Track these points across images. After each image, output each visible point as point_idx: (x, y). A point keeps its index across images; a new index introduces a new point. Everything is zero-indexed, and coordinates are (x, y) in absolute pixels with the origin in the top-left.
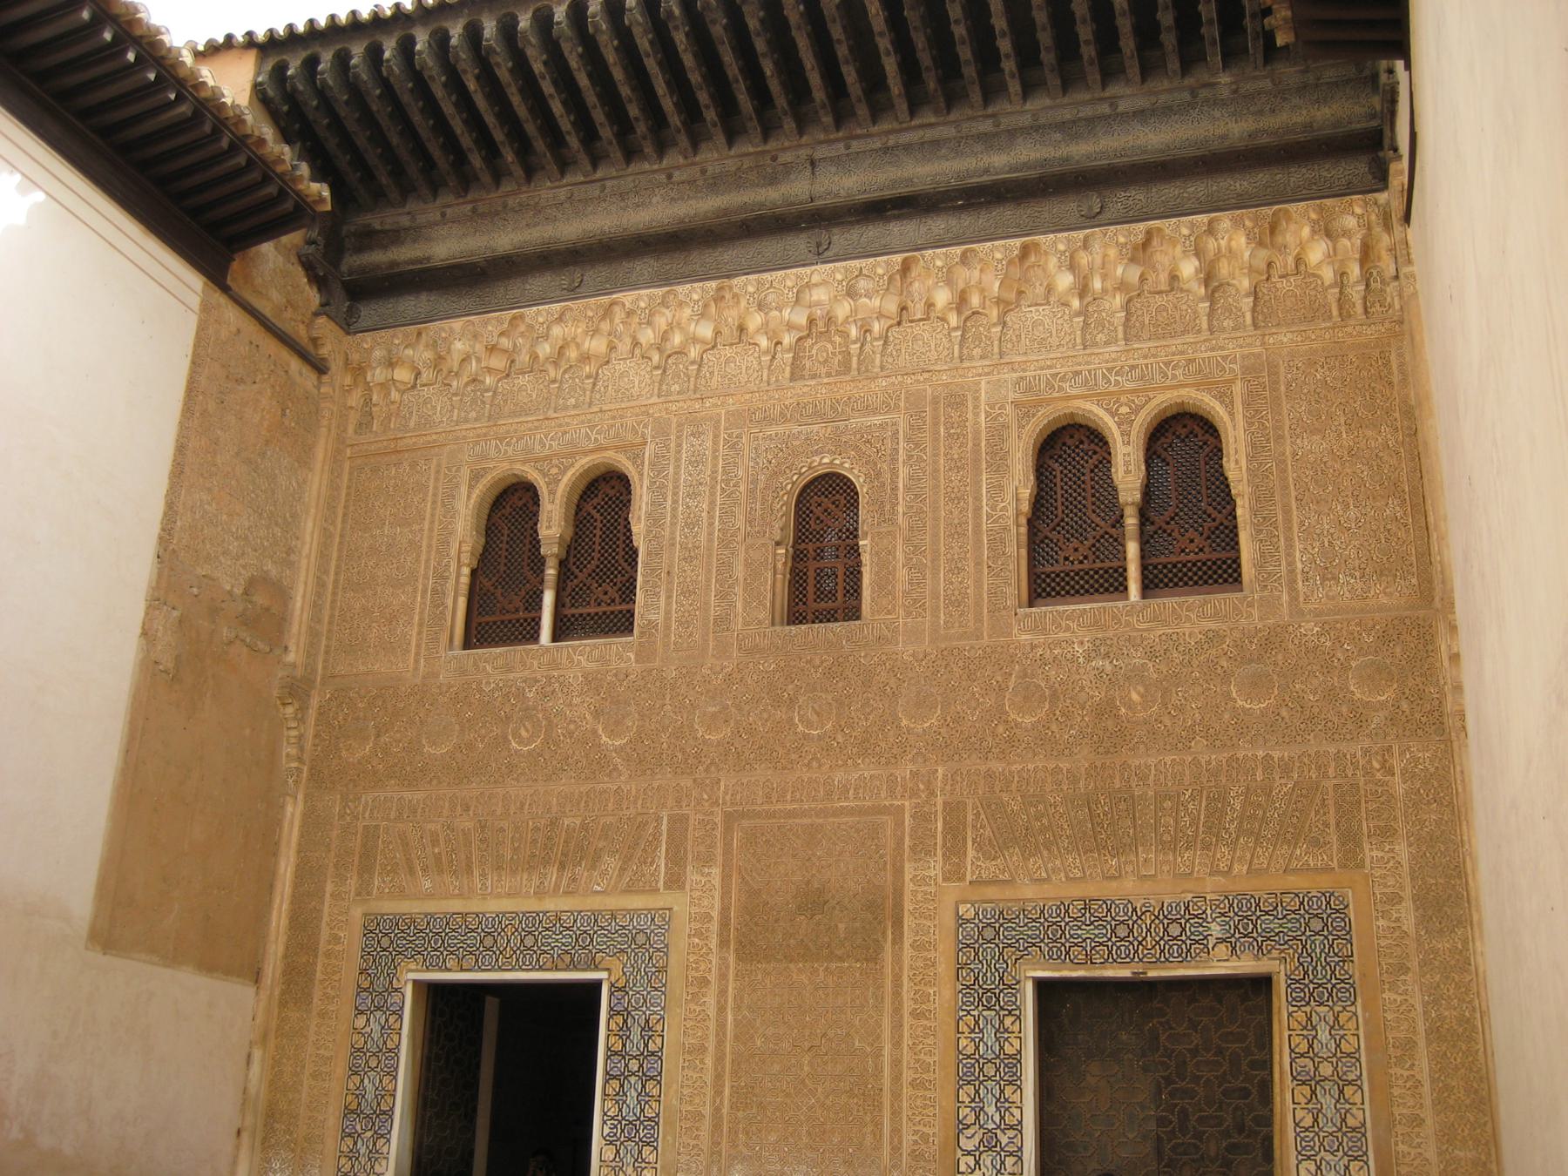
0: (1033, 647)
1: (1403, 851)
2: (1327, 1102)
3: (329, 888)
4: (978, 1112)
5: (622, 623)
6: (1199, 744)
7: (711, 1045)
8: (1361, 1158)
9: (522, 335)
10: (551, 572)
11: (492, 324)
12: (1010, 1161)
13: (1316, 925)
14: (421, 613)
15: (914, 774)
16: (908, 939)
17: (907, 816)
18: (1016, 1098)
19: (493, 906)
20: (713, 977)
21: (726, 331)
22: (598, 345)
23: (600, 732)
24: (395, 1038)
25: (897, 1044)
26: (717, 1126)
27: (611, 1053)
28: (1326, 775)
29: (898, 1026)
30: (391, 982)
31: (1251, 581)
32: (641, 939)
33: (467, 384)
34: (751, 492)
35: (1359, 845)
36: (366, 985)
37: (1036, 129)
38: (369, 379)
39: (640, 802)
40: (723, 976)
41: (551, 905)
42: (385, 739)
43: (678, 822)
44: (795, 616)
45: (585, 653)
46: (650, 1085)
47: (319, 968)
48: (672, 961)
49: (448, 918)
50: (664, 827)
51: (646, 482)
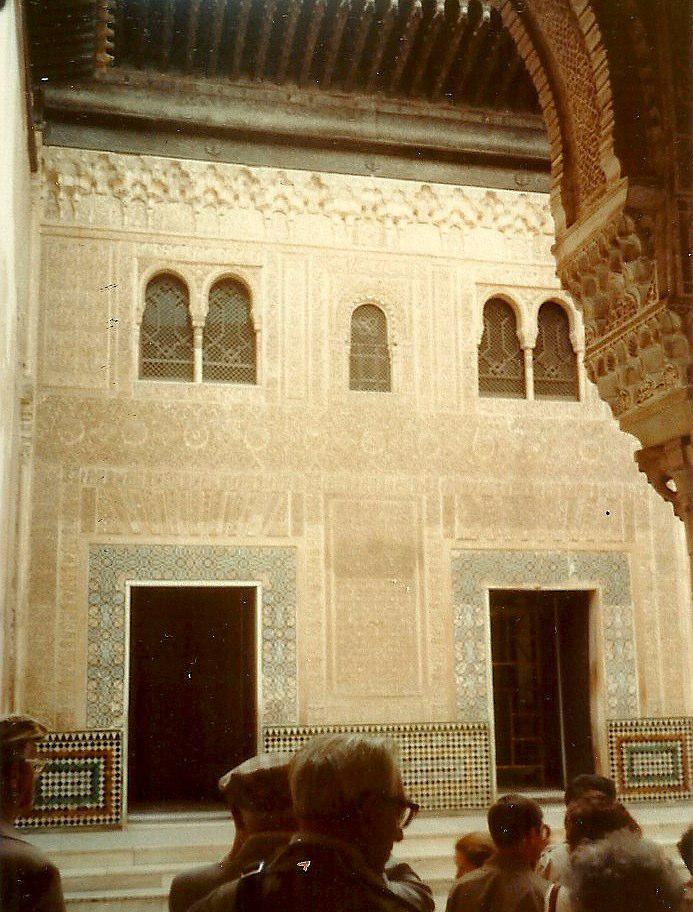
0: (486, 418)
1: (652, 535)
2: (620, 649)
3: (60, 527)
4: (465, 655)
5: (250, 376)
6: (565, 478)
7: (324, 622)
8: (632, 673)
9: (174, 176)
10: (199, 338)
11: (159, 163)
12: (481, 678)
13: (615, 568)
14: (113, 351)
15: (428, 481)
16: (427, 567)
17: (424, 503)
18: (483, 647)
19: (182, 541)
20: (323, 584)
21: (310, 205)
22: (225, 195)
23: (245, 441)
24: (121, 620)
25: (423, 623)
26: (329, 667)
27: (265, 627)
28: (620, 496)
29: (423, 611)
30: (114, 587)
31: (587, 397)
32: (279, 563)
33: (134, 200)
34: (330, 308)
35: (633, 532)
36: (96, 588)
37: (505, 128)
38: (60, 180)
39: (274, 484)
40: (328, 583)
41: (221, 542)
42: (93, 432)
43: (297, 497)
44: (353, 386)
45: (230, 393)
46: (289, 644)
47: (58, 577)
48: (299, 574)
49: (151, 548)
50: (290, 500)
51: (264, 292)
